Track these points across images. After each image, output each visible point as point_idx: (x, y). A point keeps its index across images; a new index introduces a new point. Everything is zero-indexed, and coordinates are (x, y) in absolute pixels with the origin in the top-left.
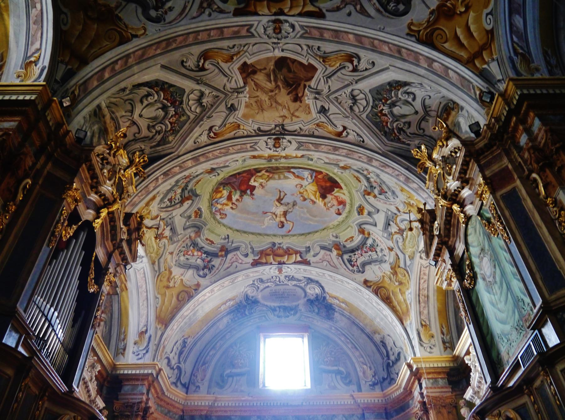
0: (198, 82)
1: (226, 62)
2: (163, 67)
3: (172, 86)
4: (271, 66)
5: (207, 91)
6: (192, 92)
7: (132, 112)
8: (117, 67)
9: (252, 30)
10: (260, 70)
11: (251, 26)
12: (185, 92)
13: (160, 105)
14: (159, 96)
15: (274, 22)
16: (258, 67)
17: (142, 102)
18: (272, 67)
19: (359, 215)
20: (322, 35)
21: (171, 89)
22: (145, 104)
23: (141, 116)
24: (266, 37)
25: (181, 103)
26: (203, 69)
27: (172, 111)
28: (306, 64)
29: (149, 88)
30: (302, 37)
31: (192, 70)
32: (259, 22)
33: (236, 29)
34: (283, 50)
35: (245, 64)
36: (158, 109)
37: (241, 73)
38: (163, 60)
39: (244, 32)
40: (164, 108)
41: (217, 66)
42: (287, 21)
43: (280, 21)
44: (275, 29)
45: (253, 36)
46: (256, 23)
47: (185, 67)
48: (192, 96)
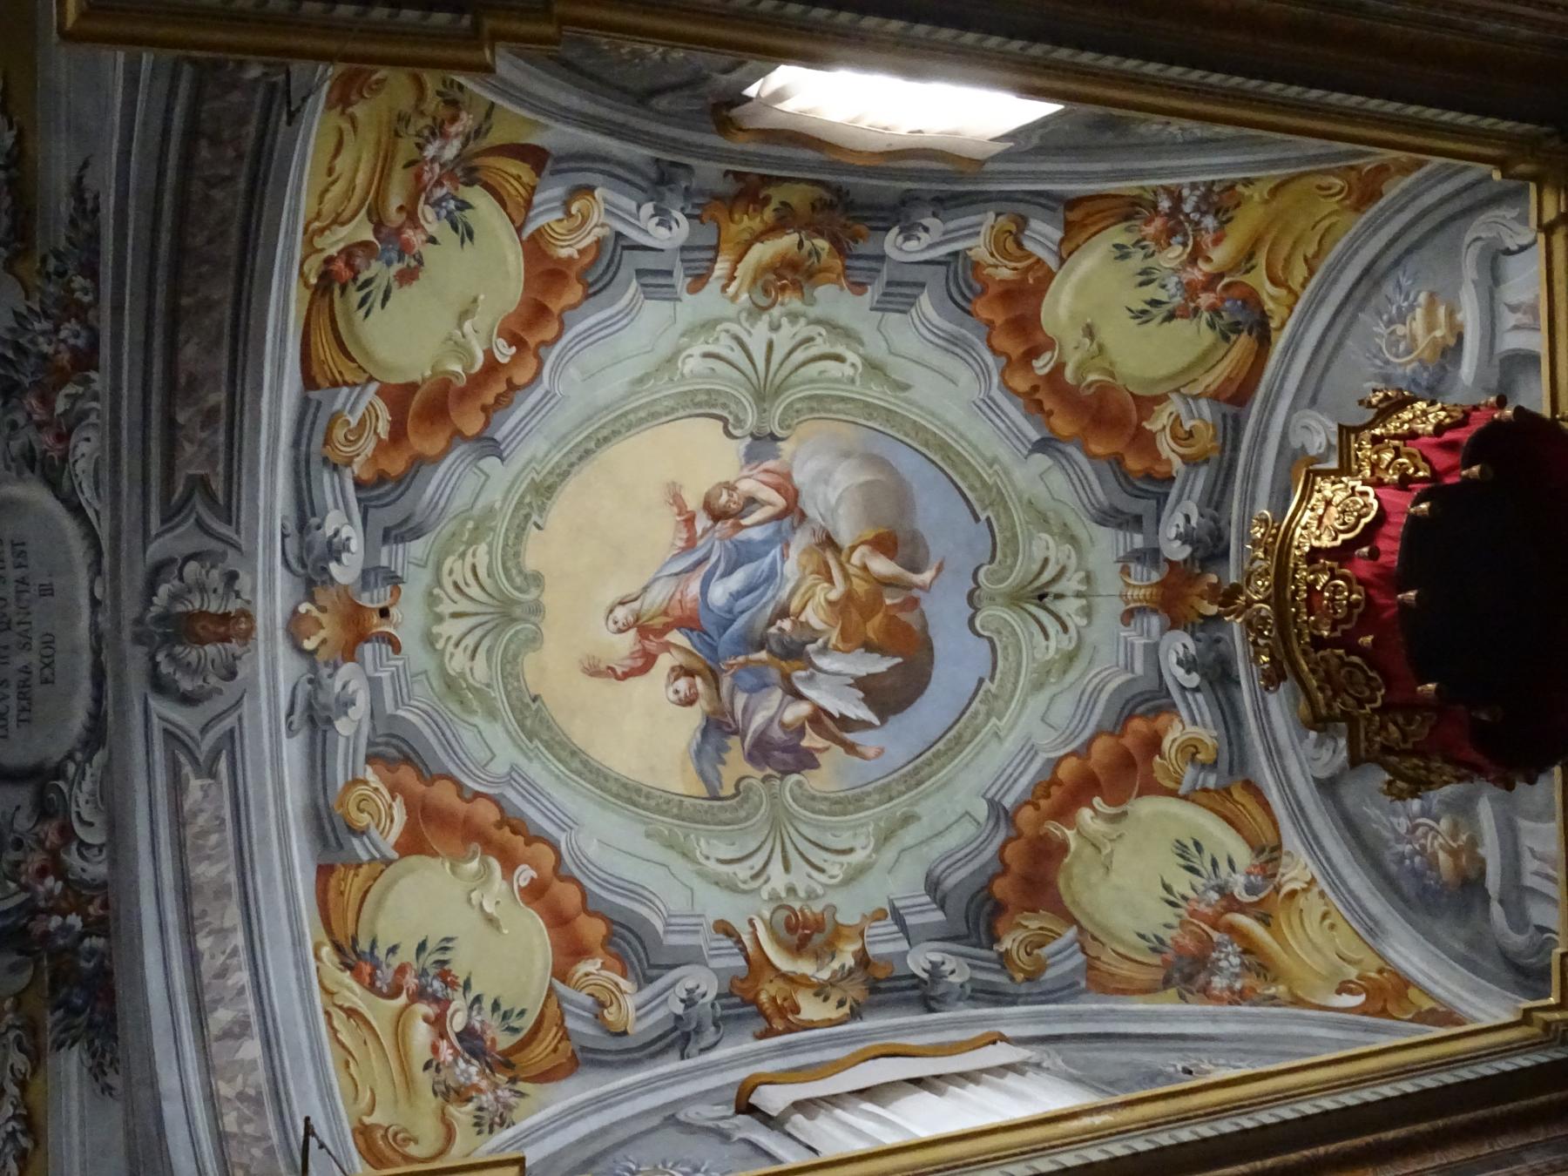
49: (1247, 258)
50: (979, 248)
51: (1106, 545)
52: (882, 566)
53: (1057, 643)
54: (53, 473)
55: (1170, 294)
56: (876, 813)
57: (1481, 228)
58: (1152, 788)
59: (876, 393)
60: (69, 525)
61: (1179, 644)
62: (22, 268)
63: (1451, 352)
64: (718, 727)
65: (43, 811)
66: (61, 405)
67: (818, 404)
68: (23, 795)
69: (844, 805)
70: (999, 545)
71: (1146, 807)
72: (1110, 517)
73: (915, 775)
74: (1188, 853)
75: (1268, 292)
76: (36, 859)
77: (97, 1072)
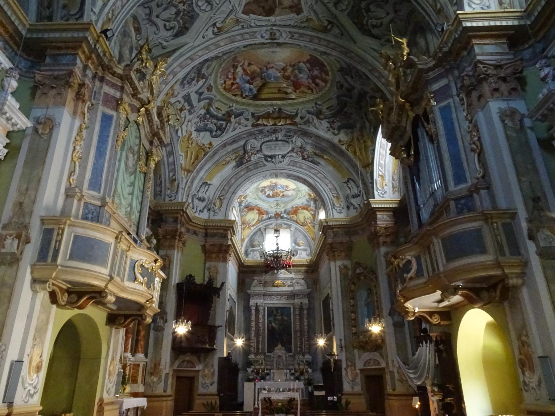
0: (335, 17)
1: (311, 19)
2: (355, 43)
3: (355, 24)
4: (277, 11)
5: (330, 5)
6: (342, 11)
7: (392, 21)
8: (377, 74)
9: (290, 36)
10: (286, 8)
11: (291, 38)
12: (348, 14)
13: (370, 14)
14: (367, 22)
15: (275, 39)
16: (287, 10)
17: (381, 24)
18: (277, 9)
19: (208, 91)
20: (242, 37)
21: (357, 21)
22: (381, 20)
23: (388, 14)
24: (281, 31)
25: (353, 7)
26: (330, 22)
27: (363, 4)
28: (251, 15)
29: (370, 31)
30: (256, 32)
31: (338, 26)
32: (285, 40)
33: (301, 39)
34: (269, 20)
35: (298, 14)
36: (374, 12)
37: (302, 8)
38: (353, 47)
39: (296, 36)
40: (368, 10)
41: (319, 20)
42: (267, 39)
43: (271, 39)
44: (275, 35)
45: (290, 32)
46: (287, 39)
47: (341, 31)
48: (344, 8)
49: (308, 226)
50: (312, 208)
51: (283, 210)
52: (281, 195)
53: (273, 206)
54: (292, 150)
55: (306, 220)
56: (257, 197)
57: (309, 249)
58: (259, 215)
59: (298, 197)
60: (286, 152)
61: (273, 215)
62: (313, 154)
63: (298, 245)
64: (265, 187)
65: (258, 151)
66: (299, 153)
67: (297, 194)
68: (259, 149)
69: (257, 195)
70: (283, 202)
71: (258, 215)
72: (285, 211)
73: (260, 199)
74: (254, 219)
75: (306, 227)
76: (253, 152)
77: (234, 167)
